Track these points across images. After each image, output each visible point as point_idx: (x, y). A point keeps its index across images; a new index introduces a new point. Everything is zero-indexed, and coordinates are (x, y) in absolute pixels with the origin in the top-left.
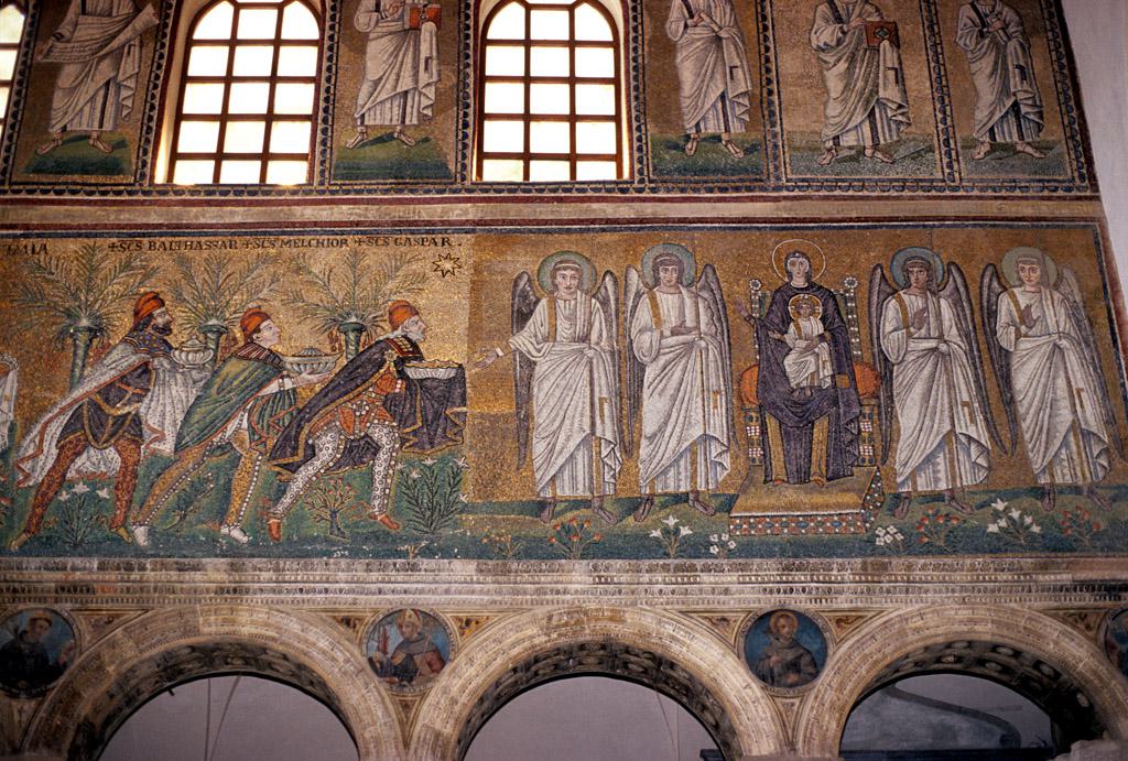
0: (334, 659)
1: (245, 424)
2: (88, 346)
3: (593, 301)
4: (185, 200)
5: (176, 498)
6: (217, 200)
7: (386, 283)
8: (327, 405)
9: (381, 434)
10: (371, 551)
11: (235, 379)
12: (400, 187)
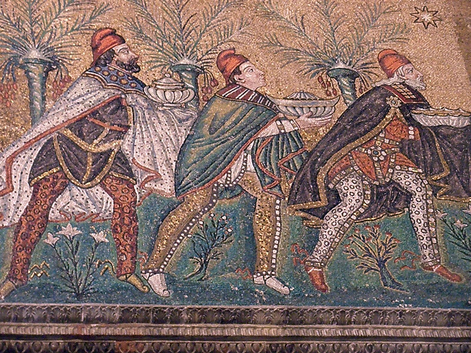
1: (251, 167)
2: (45, 78)
5: (191, 245)
8: (339, 149)
11: (225, 120)
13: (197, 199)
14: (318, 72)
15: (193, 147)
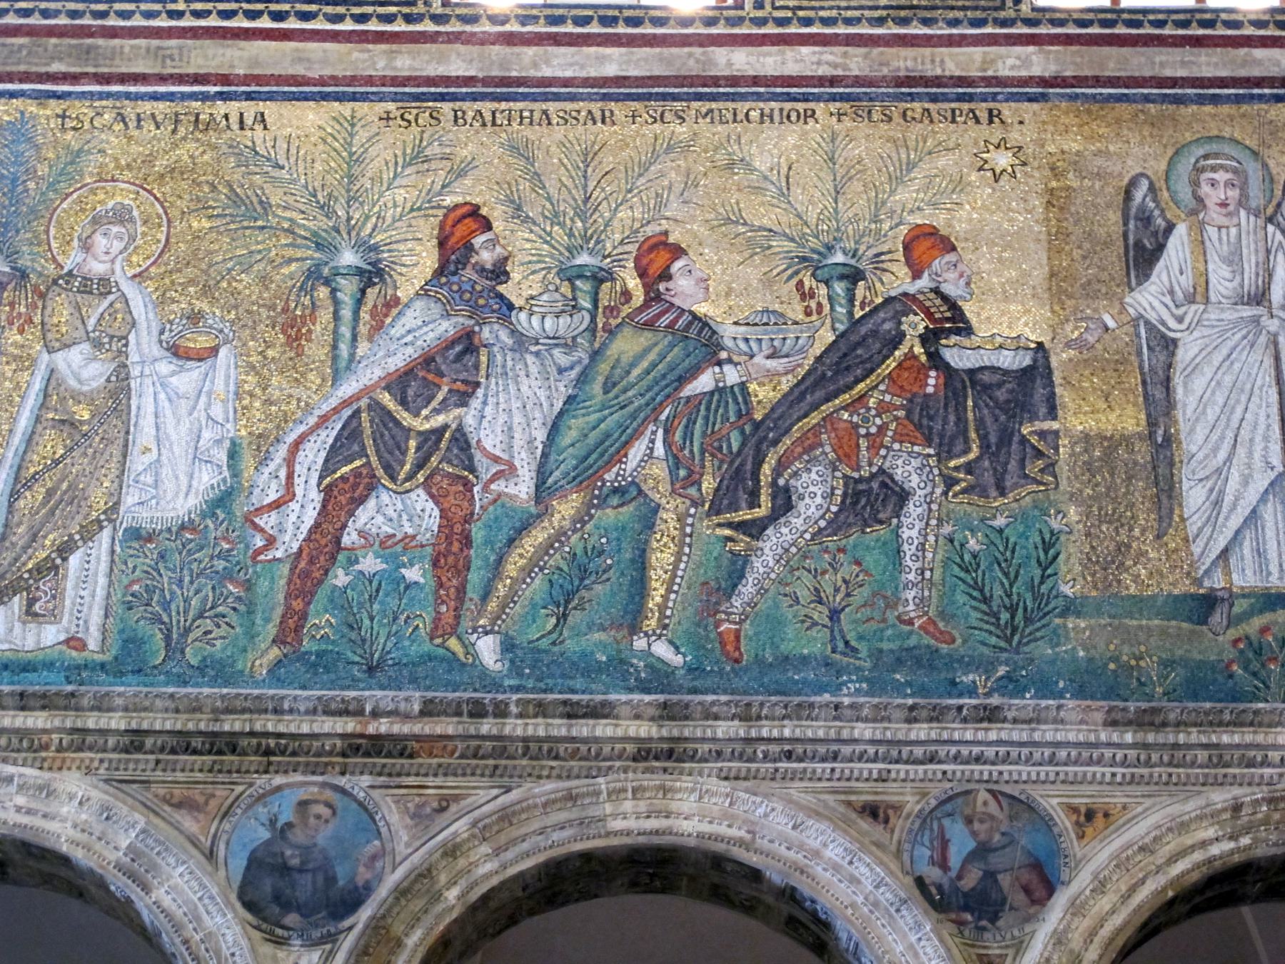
0: (854, 880)
1: (660, 450)
2: (359, 302)
3: (1270, 228)
4: (511, 34)
6: (571, 34)
7: (893, 192)
8: (806, 416)
9: (909, 467)
10: (909, 684)
11: (633, 365)
12: (903, 13)
13: (565, 509)
14: (797, 273)
15: (574, 417)
